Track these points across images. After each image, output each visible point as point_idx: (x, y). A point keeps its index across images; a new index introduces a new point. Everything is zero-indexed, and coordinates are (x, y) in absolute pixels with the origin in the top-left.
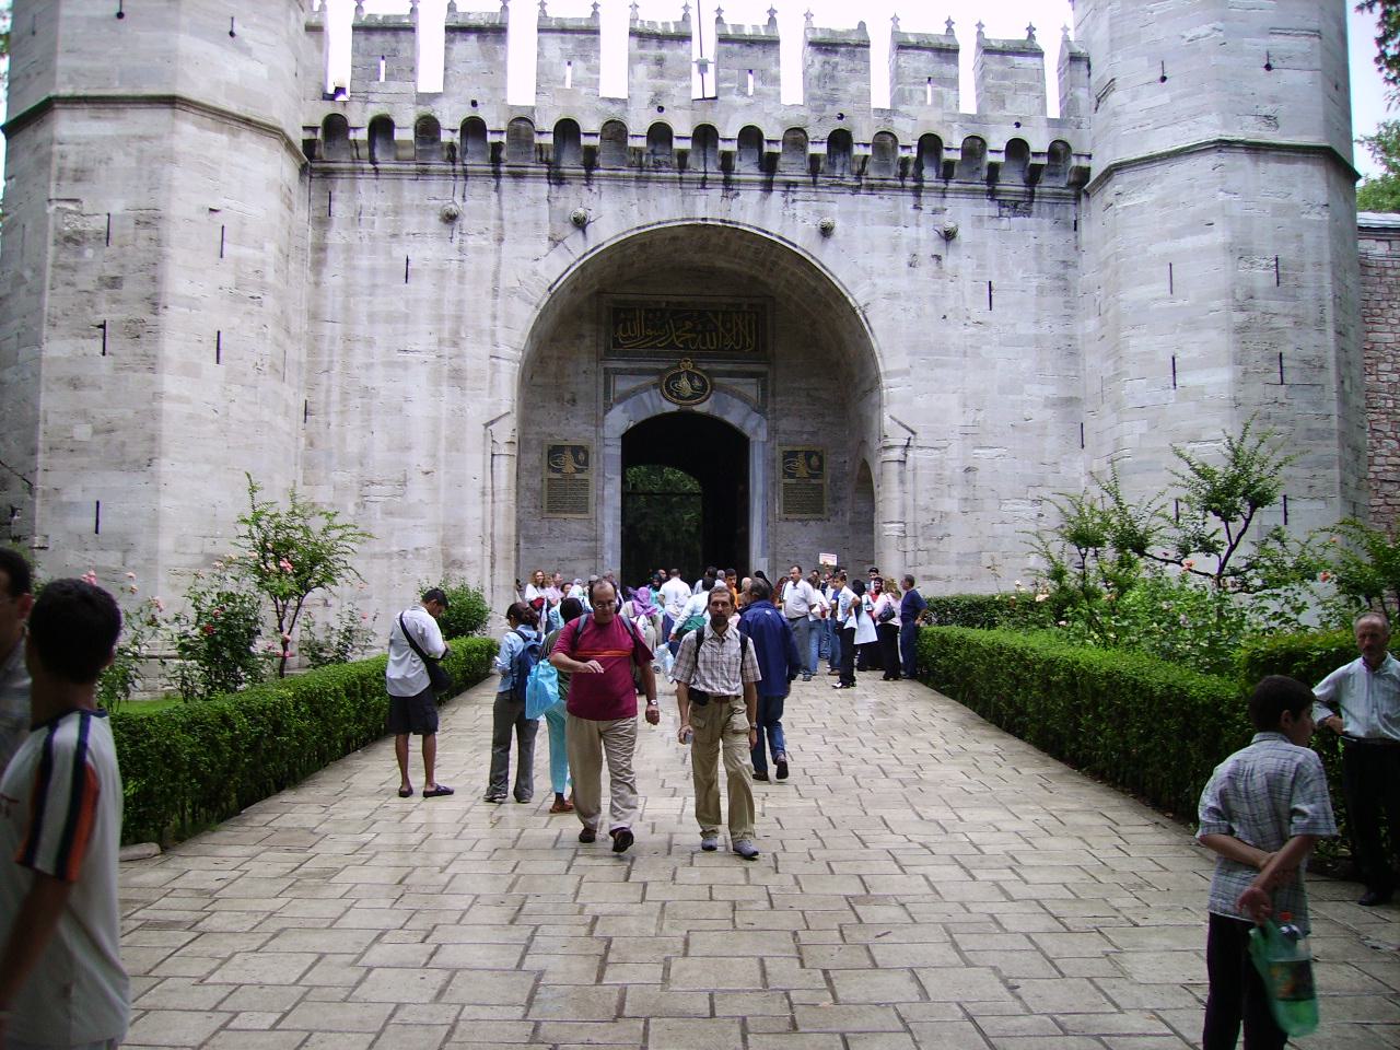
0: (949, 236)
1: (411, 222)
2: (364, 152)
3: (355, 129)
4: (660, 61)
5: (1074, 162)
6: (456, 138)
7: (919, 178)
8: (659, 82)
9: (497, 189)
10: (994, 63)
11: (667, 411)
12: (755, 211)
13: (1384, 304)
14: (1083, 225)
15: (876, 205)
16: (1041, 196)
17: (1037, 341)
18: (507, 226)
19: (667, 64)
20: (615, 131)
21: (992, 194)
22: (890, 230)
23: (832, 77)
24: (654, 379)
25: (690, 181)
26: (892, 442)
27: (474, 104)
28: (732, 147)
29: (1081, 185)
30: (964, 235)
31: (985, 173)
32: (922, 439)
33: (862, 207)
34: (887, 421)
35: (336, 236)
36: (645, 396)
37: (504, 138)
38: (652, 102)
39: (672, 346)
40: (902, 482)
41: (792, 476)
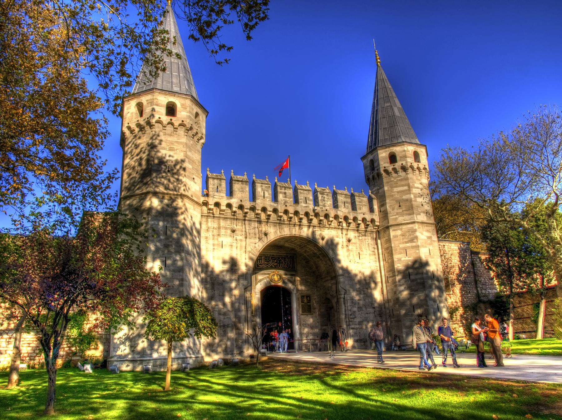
1: (223, 231)
4: (285, 193)
7: (342, 226)
9: (245, 224)
18: (248, 234)
19: (287, 194)
21: (358, 230)
23: (324, 200)
25: (292, 224)
27: (241, 201)
34: (340, 288)
38: (284, 204)
40: (344, 304)
41: (303, 302)
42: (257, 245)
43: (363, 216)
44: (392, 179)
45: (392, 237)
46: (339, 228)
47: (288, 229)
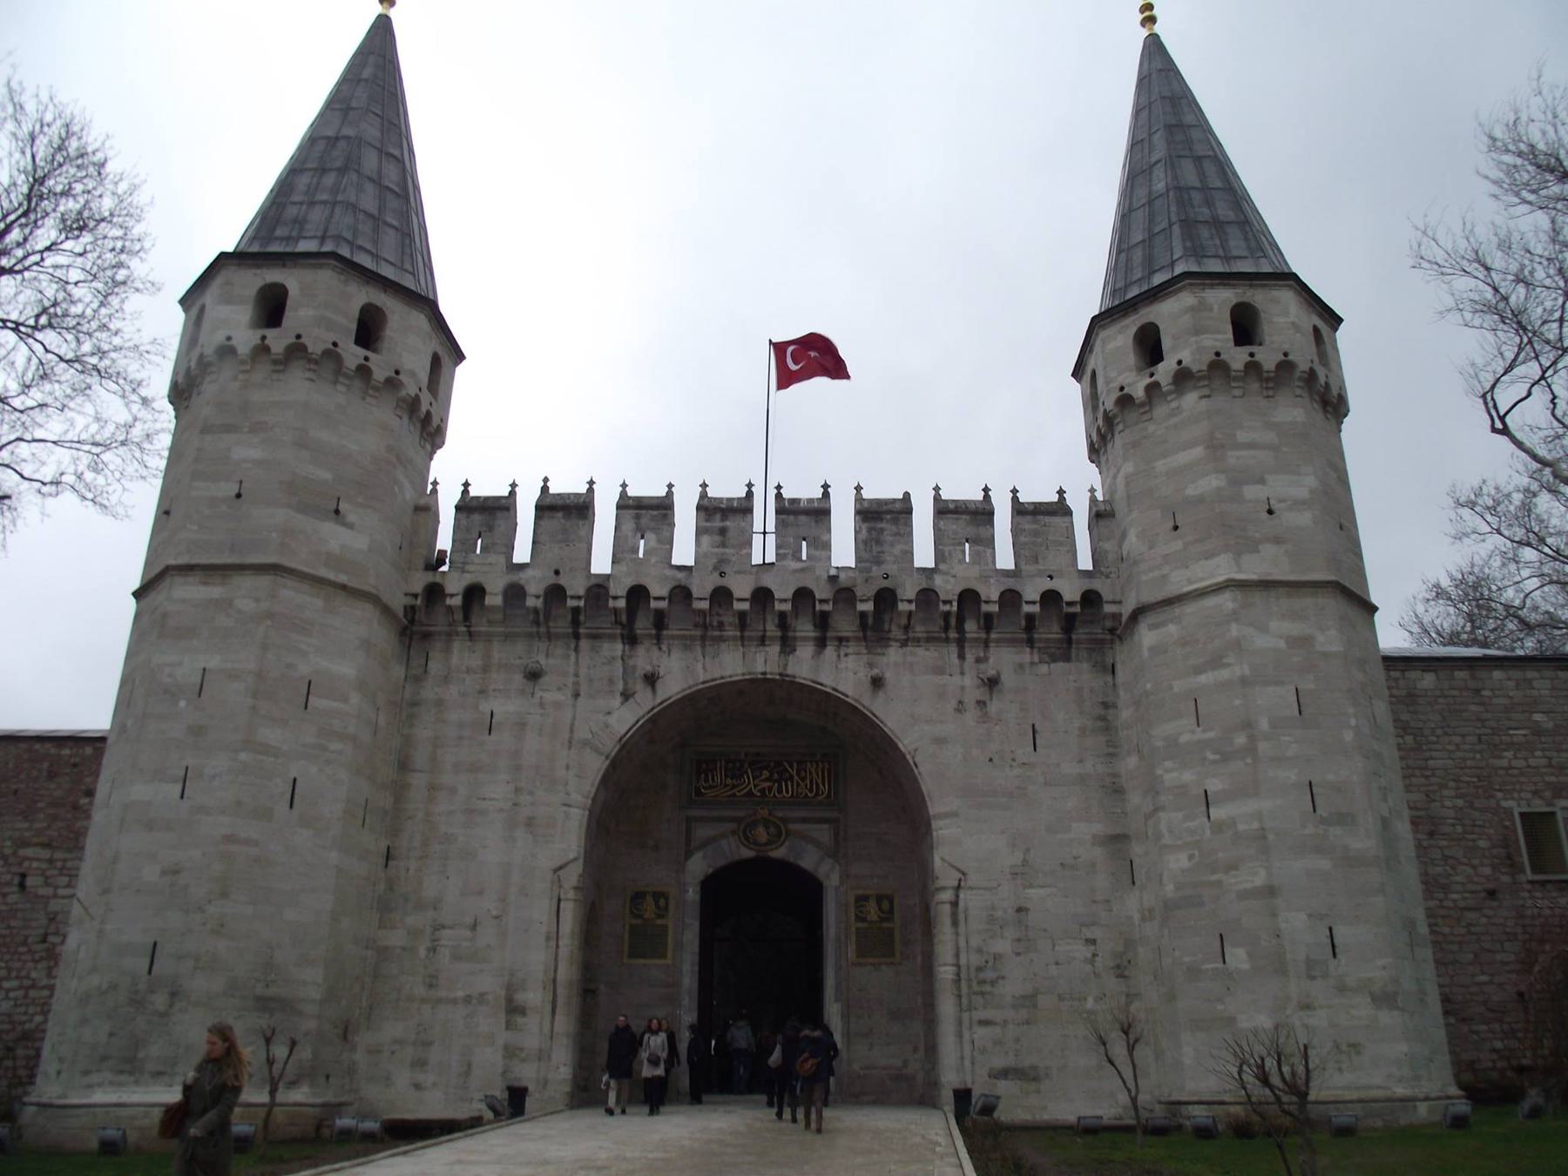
0: (992, 683)
2: (459, 616)
3: (452, 596)
4: (723, 532)
5: (1108, 609)
6: (539, 603)
7: (960, 629)
8: (721, 550)
9: (576, 650)
10: (1027, 523)
12: (806, 665)
13: (1439, 732)
14: (1118, 667)
15: (925, 655)
16: (1079, 642)
17: (1082, 780)
19: (731, 534)
20: (682, 594)
21: (1030, 642)
22: (938, 679)
23: (879, 542)
24: (734, 826)
25: (751, 639)
26: (941, 883)
27: (557, 572)
28: (787, 607)
29: (1120, 629)
30: (1008, 679)
31: (1023, 623)
32: (973, 879)
33: (909, 659)
34: (937, 862)
35: (429, 692)
37: (582, 603)
38: (715, 568)
41: (864, 920)
42: (615, 715)
43: (1048, 585)
44: (1151, 428)
45: (1146, 654)
46: (947, 640)
47: (739, 655)
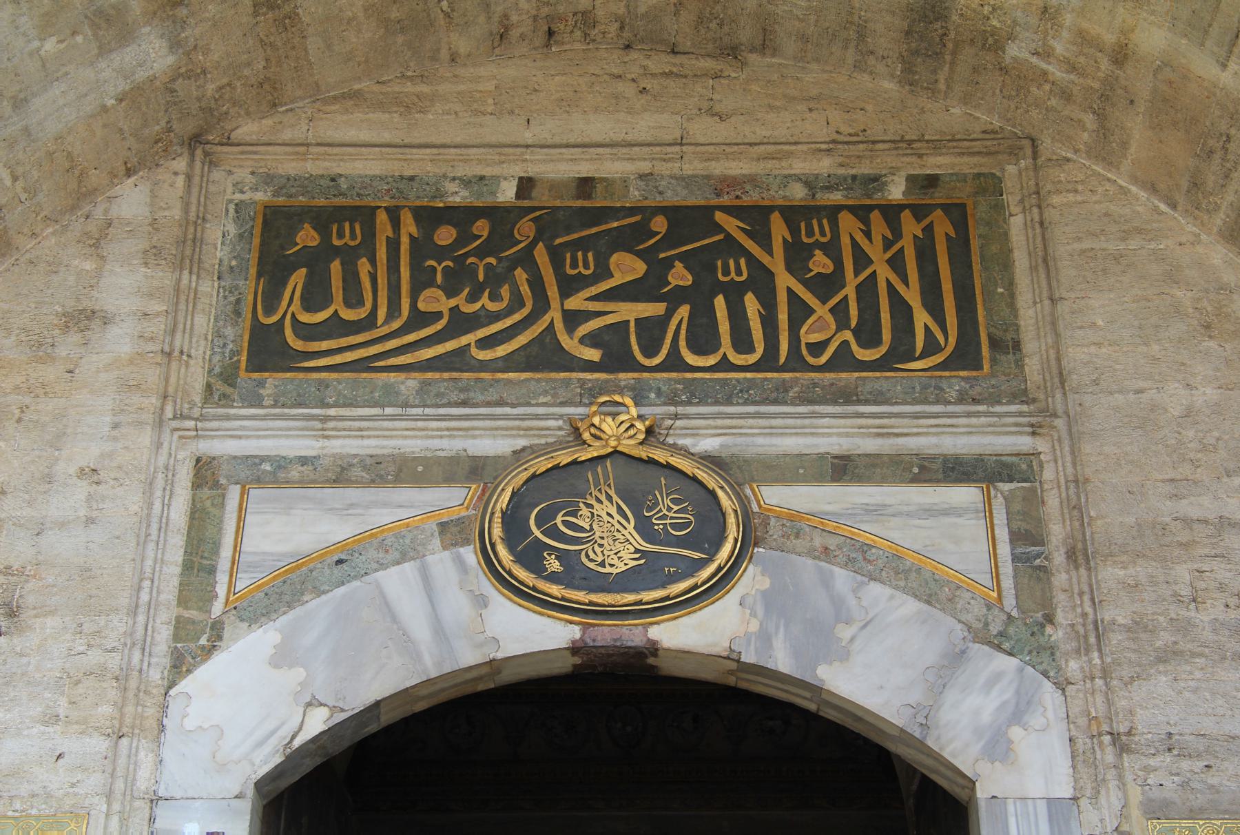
11: (511, 648)
24: (452, 499)
36: (397, 581)
39: (545, 356)
